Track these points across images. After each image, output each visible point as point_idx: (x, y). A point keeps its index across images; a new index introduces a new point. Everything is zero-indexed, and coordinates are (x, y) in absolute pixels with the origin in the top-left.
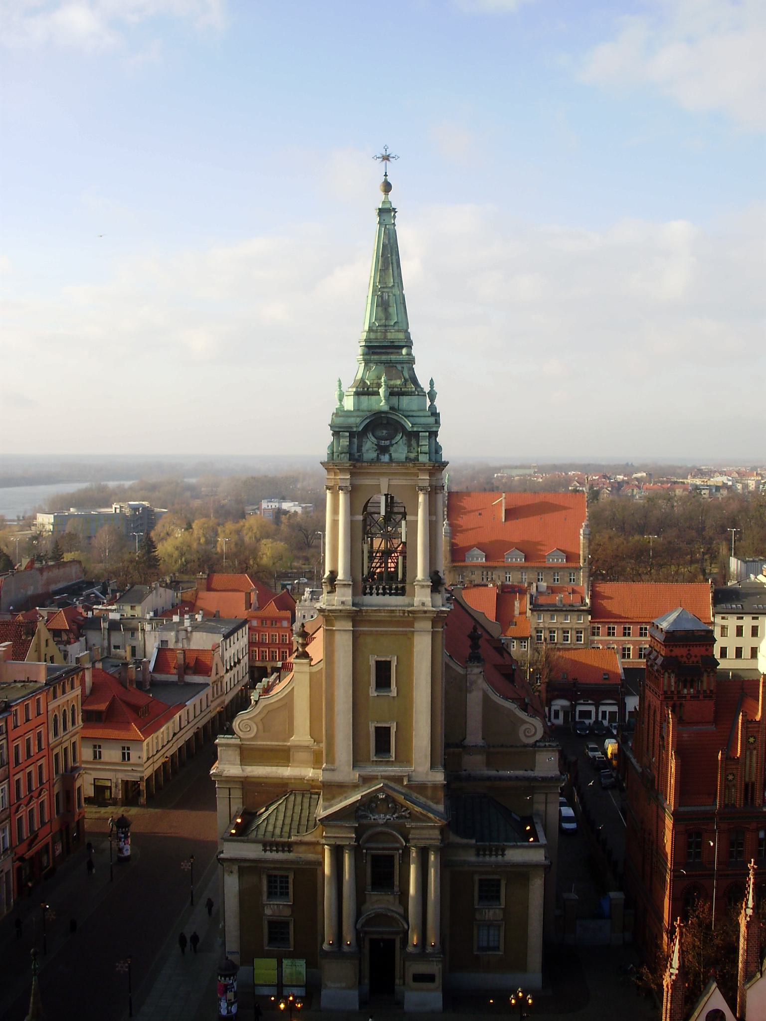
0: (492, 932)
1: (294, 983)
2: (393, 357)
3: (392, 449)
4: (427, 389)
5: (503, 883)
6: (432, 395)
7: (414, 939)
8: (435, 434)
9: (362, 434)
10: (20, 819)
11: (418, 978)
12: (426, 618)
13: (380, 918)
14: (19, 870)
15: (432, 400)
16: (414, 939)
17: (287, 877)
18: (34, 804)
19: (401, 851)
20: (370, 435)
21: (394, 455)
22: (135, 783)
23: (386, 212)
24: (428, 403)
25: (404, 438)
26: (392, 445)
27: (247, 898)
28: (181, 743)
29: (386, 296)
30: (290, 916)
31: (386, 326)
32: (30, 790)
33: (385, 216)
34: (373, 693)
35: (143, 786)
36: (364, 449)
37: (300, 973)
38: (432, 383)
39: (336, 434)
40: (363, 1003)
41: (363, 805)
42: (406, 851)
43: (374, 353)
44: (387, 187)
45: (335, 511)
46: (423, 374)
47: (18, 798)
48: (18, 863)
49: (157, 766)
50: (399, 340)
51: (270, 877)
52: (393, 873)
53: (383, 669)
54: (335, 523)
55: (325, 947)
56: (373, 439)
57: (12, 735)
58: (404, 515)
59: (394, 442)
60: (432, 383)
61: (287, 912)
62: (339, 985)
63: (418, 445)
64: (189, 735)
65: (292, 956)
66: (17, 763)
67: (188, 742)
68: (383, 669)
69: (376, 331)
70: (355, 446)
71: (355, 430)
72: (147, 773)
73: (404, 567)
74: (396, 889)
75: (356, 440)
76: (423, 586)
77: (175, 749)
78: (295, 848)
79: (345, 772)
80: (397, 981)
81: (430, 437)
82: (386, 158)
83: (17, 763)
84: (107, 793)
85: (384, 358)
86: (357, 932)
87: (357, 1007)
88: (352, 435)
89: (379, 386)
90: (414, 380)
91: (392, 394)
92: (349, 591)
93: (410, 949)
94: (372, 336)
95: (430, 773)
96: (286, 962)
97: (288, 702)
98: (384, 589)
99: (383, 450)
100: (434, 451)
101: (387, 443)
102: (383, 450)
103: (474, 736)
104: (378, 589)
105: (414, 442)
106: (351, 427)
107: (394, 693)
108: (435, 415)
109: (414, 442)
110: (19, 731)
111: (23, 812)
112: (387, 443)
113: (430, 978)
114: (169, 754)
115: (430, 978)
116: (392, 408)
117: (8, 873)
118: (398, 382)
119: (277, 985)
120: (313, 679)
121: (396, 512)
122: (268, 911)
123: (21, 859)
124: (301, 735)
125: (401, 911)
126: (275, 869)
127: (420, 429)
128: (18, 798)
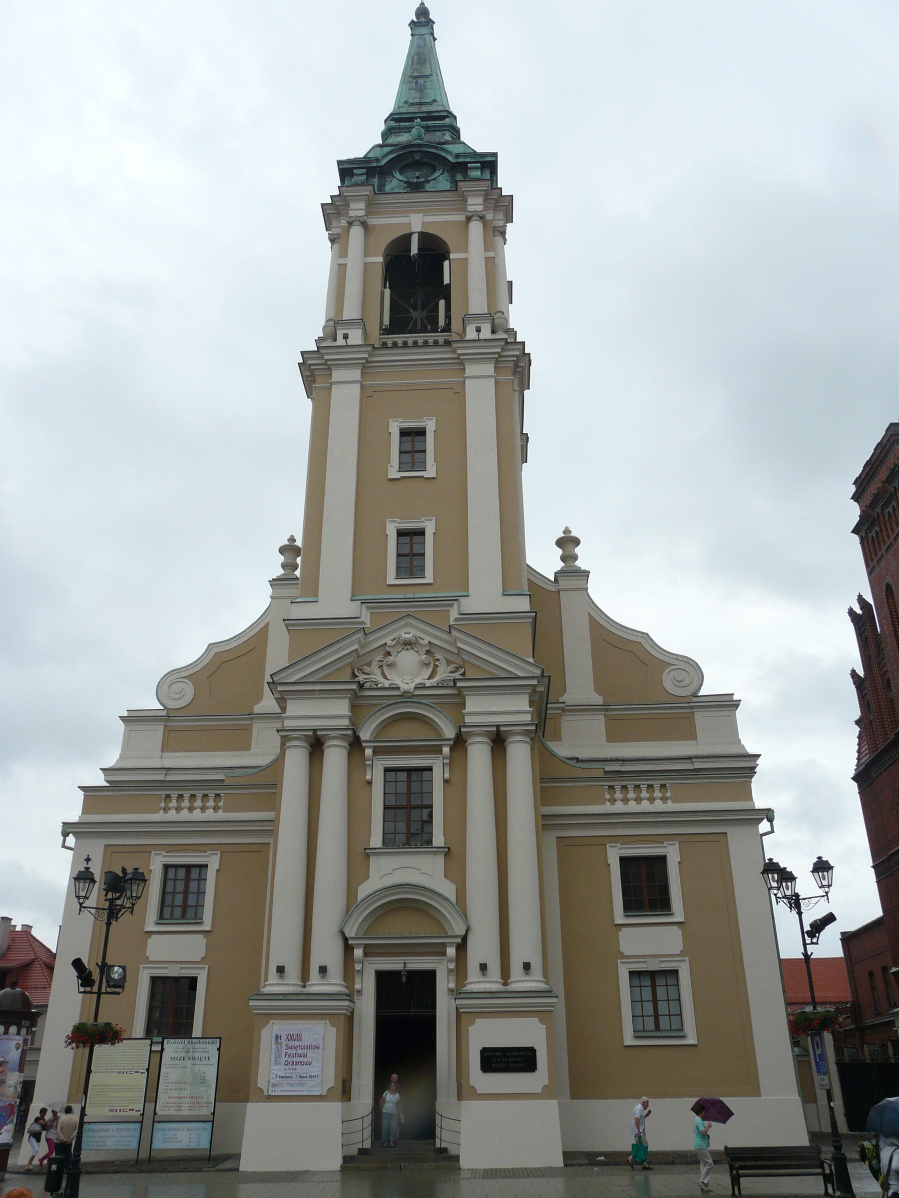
0: (661, 993)
1: (185, 1112)
12: (478, 359)
19: (446, 750)
20: (397, 175)
25: (446, 174)
30: (203, 960)
31: (420, 104)
37: (203, 1081)
53: (413, 436)
68: (413, 436)
71: (374, 164)
74: (438, 839)
86: (348, 949)
87: (336, 1163)
99: (415, 187)
107: (431, 471)
125: (448, 889)
127: (468, 160)
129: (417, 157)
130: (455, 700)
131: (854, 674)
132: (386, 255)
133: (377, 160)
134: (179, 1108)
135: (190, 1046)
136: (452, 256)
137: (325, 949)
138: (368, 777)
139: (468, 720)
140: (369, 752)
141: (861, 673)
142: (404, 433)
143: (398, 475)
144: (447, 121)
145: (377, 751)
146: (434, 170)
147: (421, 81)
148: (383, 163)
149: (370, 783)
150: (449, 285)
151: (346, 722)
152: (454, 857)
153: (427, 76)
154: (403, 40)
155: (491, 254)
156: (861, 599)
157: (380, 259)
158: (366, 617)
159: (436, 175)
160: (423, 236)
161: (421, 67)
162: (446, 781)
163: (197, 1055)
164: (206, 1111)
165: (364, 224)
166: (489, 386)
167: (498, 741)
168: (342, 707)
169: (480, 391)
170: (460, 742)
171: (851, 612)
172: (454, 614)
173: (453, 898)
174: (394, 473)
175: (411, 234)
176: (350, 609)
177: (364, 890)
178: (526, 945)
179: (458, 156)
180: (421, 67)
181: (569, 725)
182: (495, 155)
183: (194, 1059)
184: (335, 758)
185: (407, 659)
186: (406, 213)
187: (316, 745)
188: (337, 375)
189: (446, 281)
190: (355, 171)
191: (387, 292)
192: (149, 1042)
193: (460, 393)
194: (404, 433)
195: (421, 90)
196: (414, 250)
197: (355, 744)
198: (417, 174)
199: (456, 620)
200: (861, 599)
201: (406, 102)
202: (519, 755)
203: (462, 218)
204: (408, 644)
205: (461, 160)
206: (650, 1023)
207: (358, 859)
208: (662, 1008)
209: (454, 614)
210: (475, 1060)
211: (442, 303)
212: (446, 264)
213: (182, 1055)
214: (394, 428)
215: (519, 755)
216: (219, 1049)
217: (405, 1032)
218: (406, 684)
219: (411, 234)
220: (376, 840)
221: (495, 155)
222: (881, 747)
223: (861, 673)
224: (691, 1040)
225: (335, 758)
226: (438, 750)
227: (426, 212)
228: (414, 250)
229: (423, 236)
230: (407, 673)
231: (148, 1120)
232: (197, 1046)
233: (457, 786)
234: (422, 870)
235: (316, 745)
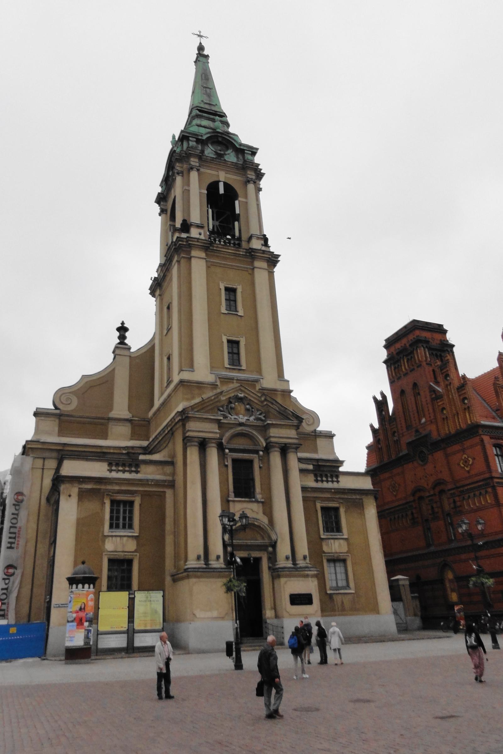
1: (148, 628)
3: (226, 158)
5: (342, 511)
12: (262, 259)
17: (131, 503)
20: (210, 146)
25: (234, 153)
26: (226, 154)
27: (86, 529)
30: (136, 551)
31: (210, 104)
37: (156, 612)
41: (222, 407)
51: (113, 502)
52: (253, 480)
59: (226, 153)
61: (131, 546)
62: (209, 614)
71: (200, 138)
73: (240, 231)
76: (258, 238)
78: (143, 468)
80: (268, 613)
94: (202, 105)
95: (279, 382)
98: (224, 242)
104: (220, 241)
105: (240, 157)
106: (197, 135)
107: (241, 313)
112: (222, 152)
119: (127, 632)
122: (109, 546)
126: (119, 492)
127: (245, 148)
129: (220, 139)
130: (264, 429)
131: (372, 426)
132: (207, 190)
133: (202, 136)
134: (146, 626)
135: (148, 595)
136: (240, 199)
138: (226, 463)
139: (273, 440)
140: (227, 451)
141: (376, 426)
142: (227, 289)
143: (226, 312)
144: (223, 119)
145: (231, 450)
146: (227, 149)
147: (208, 90)
148: (205, 137)
149: (227, 466)
150: (239, 214)
151: (218, 436)
153: (210, 89)
156: (383, 395)
157: (206, 192)
158: (218, 383)
159: (229, 151)
160: (226, 184)
161: (204, 81)
162: (260, 467)
163: (152, 599)
164: (159, 627)
165: (198, 170)
166: (265, 274)
168: (214, 428)
169: (260, 276)
170: (267, 449)
171: (375, 398)
172: (258, 387)
174: (224, 310)
175: (220, 181)
176: (210, 378)
180: (204, 81)
182: (257, 149)
183: (151, 601)
186: (217, 170)
187: (203, 445)
188: (194, 253)
189: (237, 212)
190: (190, 138)
191: (210, 211)
192: (127, 593)
193: (252, 274)
194: (227, 289)
195: (209, 96)
196: (222, 191)
197: (221, 447)
198: (219, 148)
199: (260, 389)
200: (383, 395)
201: (202, 101)
203: (245, 179)
204: (240, 400)
205: (242, 147)
209: (258, 387)
211: (236, 223)
212: (237, 203)
213: (145, 599)
214: (222, 287)
216: (163, 596)
219: (220, 181)
220: (232, 494)
221: (257, 149)
222: (386, 460)
223: (376, 426)
226: (257, 452)
227: (227, 172)
228: (222, 191)
231: (131, 633)
232: (151, 594)
234: (253, 510)
235: (203, 445)
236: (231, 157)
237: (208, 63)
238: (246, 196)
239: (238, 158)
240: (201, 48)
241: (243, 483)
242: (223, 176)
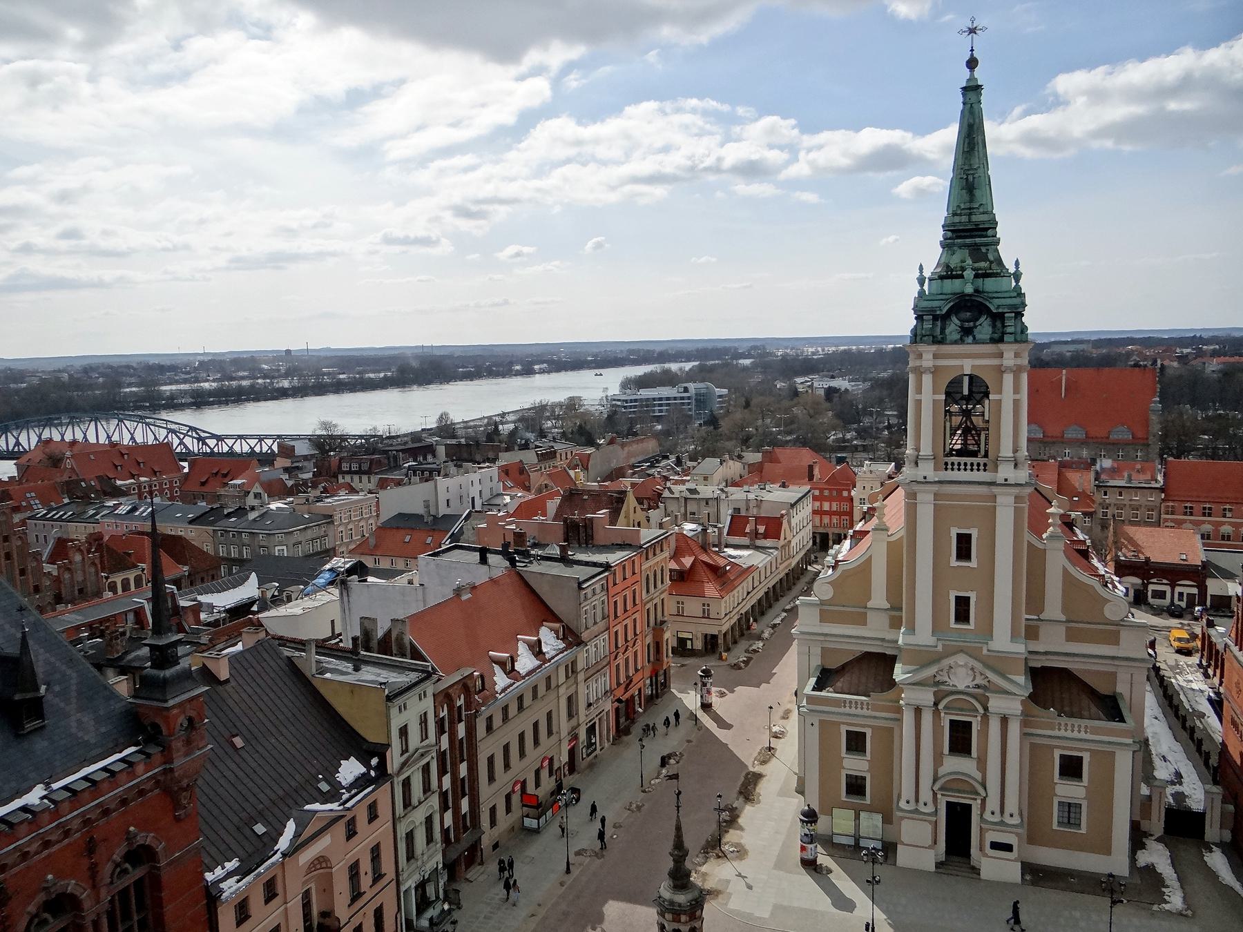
2: (978, 240)
3: (976, 331)
4: (1012, 270)
6: (1017, 276)
7: (993, 803)
8: (1019, 315)
9: (945, 318)
10: (618, 666)
11: (995, 846)
13: (957, 783)
14: (617, 710)
15: (1017, 281)
16: (993, 803)
18: (630, 653)
20: (954, 319)
21: (978, 336)
22: (714, 637)
23: (972, 90)
24: (1014, 284)
28: (754, 601)
29: (971, 178)
32: (626, 641)
33: (971, 95)
34: (954, 562)
35: (721, 641)
36: (947, 331)
38: (1017, 264)
39: (919, 318)
40: (939, 865)
42: (985, 717)
43: (958, 237)
44: (972, 63)
45: (919, 390)
46: (1008, 252)
47: (617, 647)
48: (616, 704)
49: (733, 622)
50: (983, 222)
54: (918, 403)
55: (903, 804)
56: (957, 322)
57: (611, 593)
58: (987, 395)
60: (1017, 264)
63: (1004, 326)
64: (761, 594)
65: (871, 809)
66: (616, 617)
67: (760, 601)
69: (960, 215)
70: (938, 330)
72: (726, 627)
75: (939, 323)
77: (748, 607)
79: (924, 635)
81: (1016, 318)
82: (972, 31)
83: (616, 617)
84: (689, 643)
85: (968, 241)
86: (935, 794)
87: (933, 869)
88: (935, 318)
89: (963, 269)
90: (999, 261)
91: (976, 276)
92: (931, 465)
93: (987, 816)
94: (957, 219)
96: (862, 814)
97: (865, 568)
99: (966, 332)
100: (1019, 330)
101: (971, 324)
102: (966, 332)
103: (1053, 608)
105: (999, 324)
108: (1020, 295)
109: (999, 324)
110: (618, 589)
111: (621, 660)
113: (1008, 848)
114: (743, 611)
115: (1008, 848)
116: (976, 291)
117: (608, 713)
118: (983, 264)
120: (894, 548)
121: (978, 390)
123: (619, 701)
124: (879, 598)
125: (978, 776)
128: (617, 647)
137: (926, 795)
152: (982, 764)
154: (956, 103)
155: (1017, 397)
159: (982, 319)
167: (1004, 720)
173: (979, 779)
177: (941, 771)
178: (1012, 804)
179: (999, 307)
181: (1044, 630)
184: (927, 718)
185: (962, 672)
202: (1014, 729)
206: (1066, 820)
207: (938, 760)
208: (1072, 815)
210: (988, 845)
215: (1014, 729)
217: (958, 821)
218: (961, 687)
224: (1083, 831)
225: (927, 718)
229: (971, 377)
230: (961, 680)
233: (984, 733)
235: (918, 711)
236: (984, 328)
237: (980, 102)
238: (1000, 392)
239: (994, 326)
240: (972, 63)
241: (960, 739)
242: (968, 367)
